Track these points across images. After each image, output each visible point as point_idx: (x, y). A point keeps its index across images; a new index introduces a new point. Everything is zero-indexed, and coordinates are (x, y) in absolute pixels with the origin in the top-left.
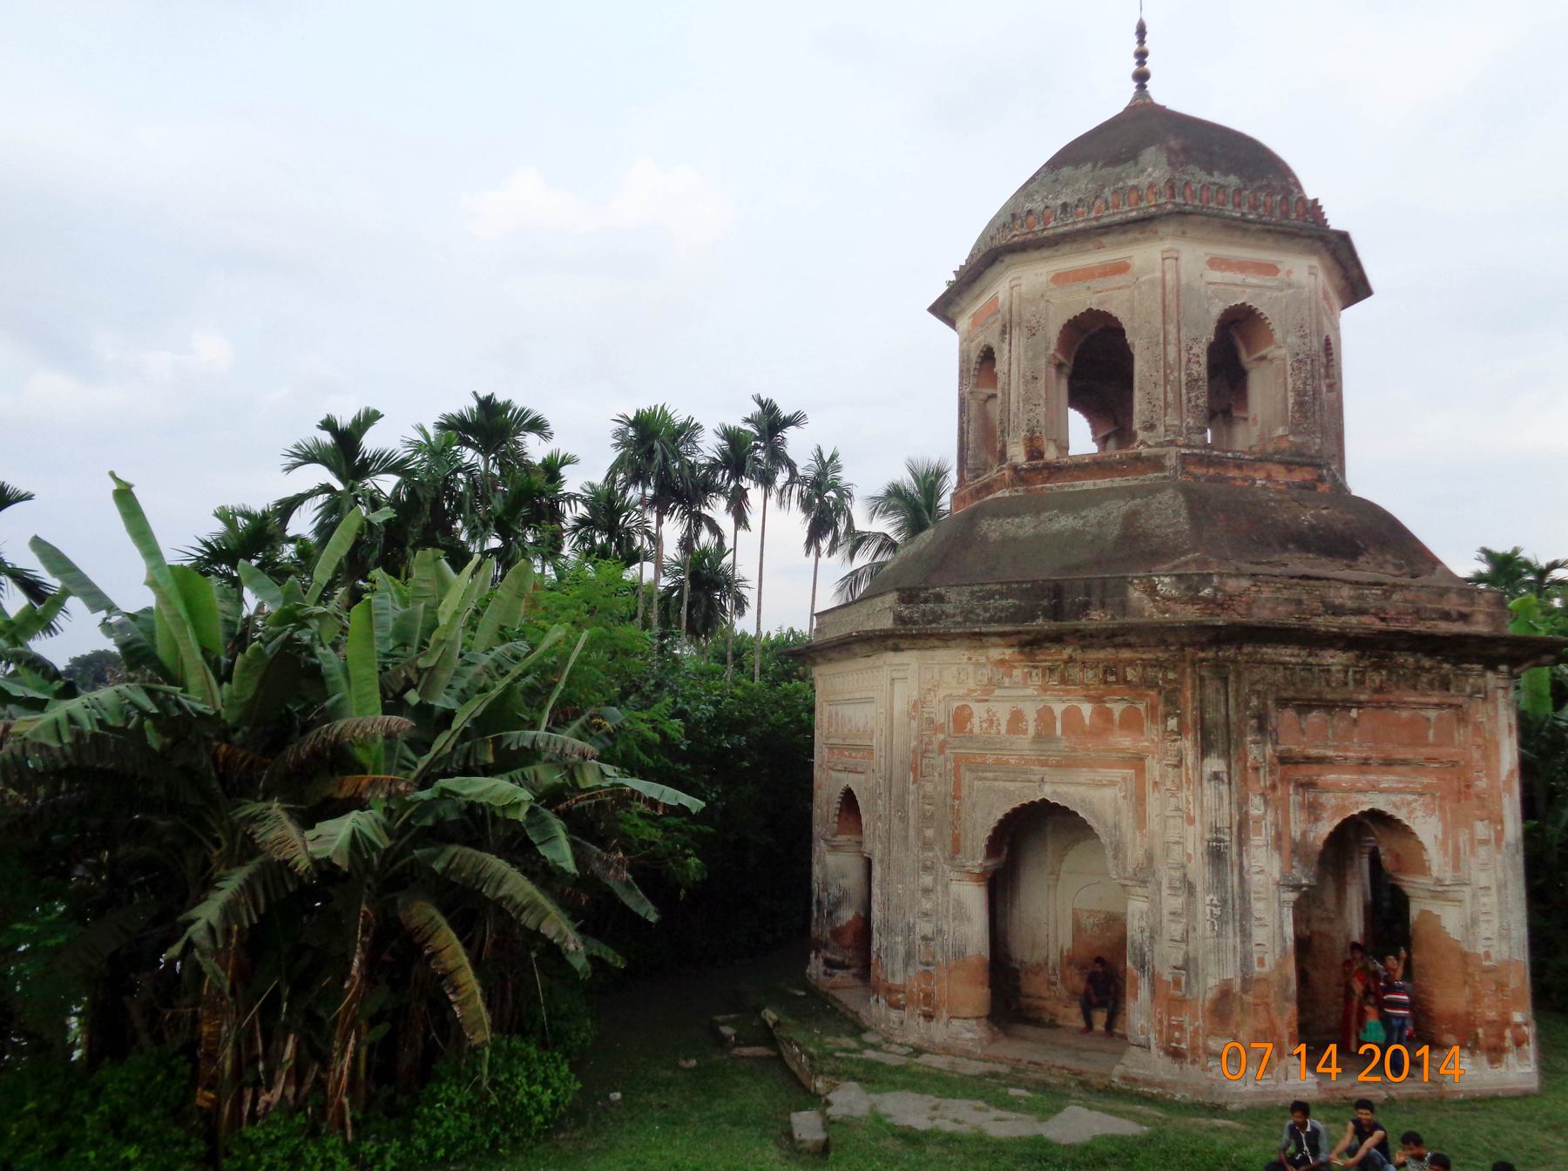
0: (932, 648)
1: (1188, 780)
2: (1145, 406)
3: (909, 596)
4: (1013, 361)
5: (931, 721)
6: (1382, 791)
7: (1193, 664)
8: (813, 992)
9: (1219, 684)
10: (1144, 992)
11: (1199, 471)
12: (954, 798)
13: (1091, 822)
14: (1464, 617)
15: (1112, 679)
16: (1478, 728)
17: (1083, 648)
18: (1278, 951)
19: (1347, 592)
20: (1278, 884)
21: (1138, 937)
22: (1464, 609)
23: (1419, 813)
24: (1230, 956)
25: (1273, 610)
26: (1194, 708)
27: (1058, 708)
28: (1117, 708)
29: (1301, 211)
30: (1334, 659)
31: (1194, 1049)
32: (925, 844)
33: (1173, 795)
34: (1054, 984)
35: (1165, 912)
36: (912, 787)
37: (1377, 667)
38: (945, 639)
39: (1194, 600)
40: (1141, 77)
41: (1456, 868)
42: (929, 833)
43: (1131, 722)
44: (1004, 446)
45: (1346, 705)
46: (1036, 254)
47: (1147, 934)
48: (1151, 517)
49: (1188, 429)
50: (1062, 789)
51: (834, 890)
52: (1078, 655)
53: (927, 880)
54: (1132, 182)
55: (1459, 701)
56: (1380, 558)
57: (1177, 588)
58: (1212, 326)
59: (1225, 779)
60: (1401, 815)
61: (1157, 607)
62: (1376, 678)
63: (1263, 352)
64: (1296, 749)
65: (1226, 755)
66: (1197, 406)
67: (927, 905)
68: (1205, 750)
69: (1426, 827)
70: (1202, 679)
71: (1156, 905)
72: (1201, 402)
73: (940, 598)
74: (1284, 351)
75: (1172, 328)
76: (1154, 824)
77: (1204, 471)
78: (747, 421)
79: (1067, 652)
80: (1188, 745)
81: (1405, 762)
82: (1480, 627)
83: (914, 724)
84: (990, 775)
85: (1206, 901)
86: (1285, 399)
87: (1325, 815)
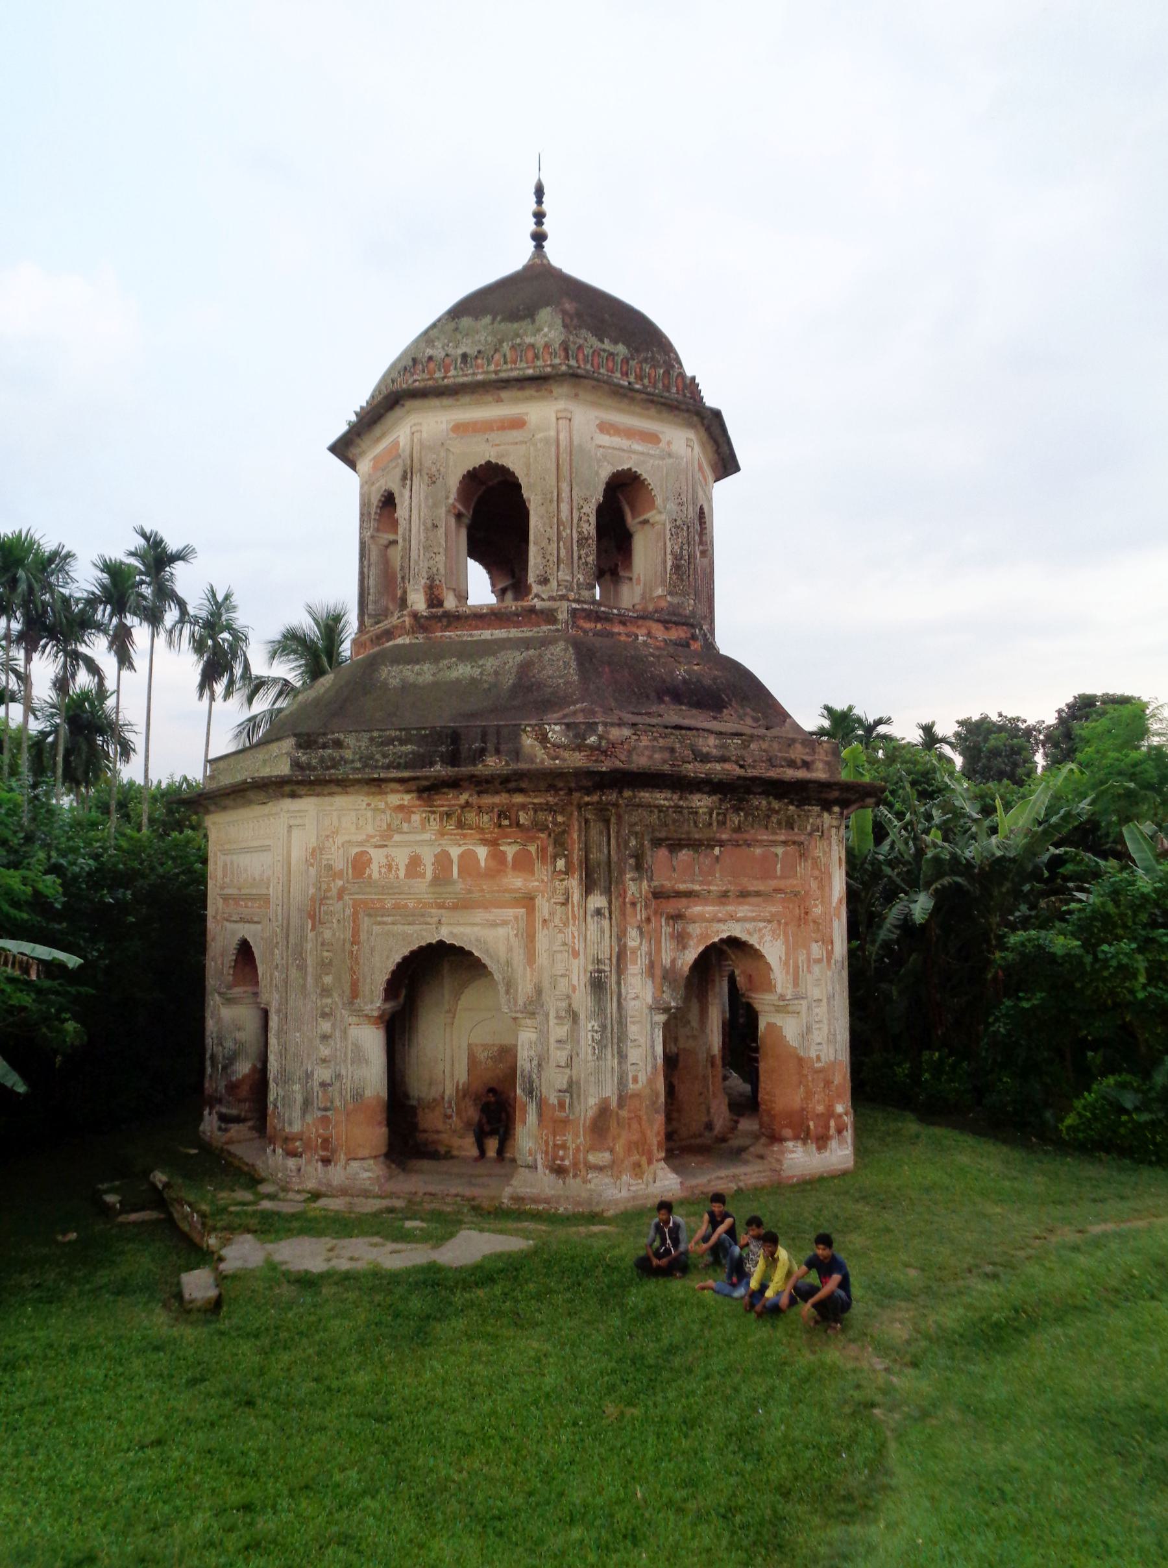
0: (331, 794)
1: (574, 916)
2: (539, 560)
3: (306, 742)
4: (413, 508)
5: (330, 867)
6: (738, 920)
7: (579, 807)
8: (206, 1148)
9: (601, 825)
10: (532, 1117)
11: (588, 625)
12: (353, 943)
13: (486, 960)
14: (806, 765)
15: (506, 822)
16: (815, 861)
17: (479, 793)
18: (649, 1069)
19: (713, 740)
20: (651, 1008)
21: (527, 1066)
22: (808, 758)
23: (768, 938)
24: (609, 1075)
25: (650, 757)
26: (580, 849)
27: (455, 852)
28: (510, 851)
29: (681, 385)
30: (701, 802)
31: (575, 1164)
32: (323, 990)
33: (560, 931)
34: (450, 1117)
35: (552, 1040)
36: (311, 935)
37: (737, 810)
38: (343, 785)
39: (579, 748)
40: (539, 238)
41: (796, 984)
42: (328, 980)
43: (523, 864)
44: (405, 592)
46: (436, 402)
47: (535, 1062)
48: (544, 668)
49: (578, 585)
50: (458, 930)
51: (229, 1044)
52: (474, 800)
53: (326, 1026)
54: (529, 340)
55: (802, 838)
56: (741, 711)
57: (567, 736)
58: (601, 488)
59: (607, 915)
60: (753, 940)
61: (548, 754)
62: (735, 819)
63: (645, 517)
64: (668, 884)
65: (608, 892)
66: (587, 563)
67: (325, 1051)
68: (588, 890)
70: (587, 821)
71: (543, 1034)
72: (590, 559)
73: (338, 744)
74: (663, 517)
75: (565, 487)
76: (542, 959)
77: (593, 625)
78: (132, 554)
79: (464, 797)
80: (574, 884)
81: (758, 894)
82: (820, 774)
83: (312, 871)
84: (389, 919)
85: (587, 1026)
86: (665, 562)
87: (692, 943)
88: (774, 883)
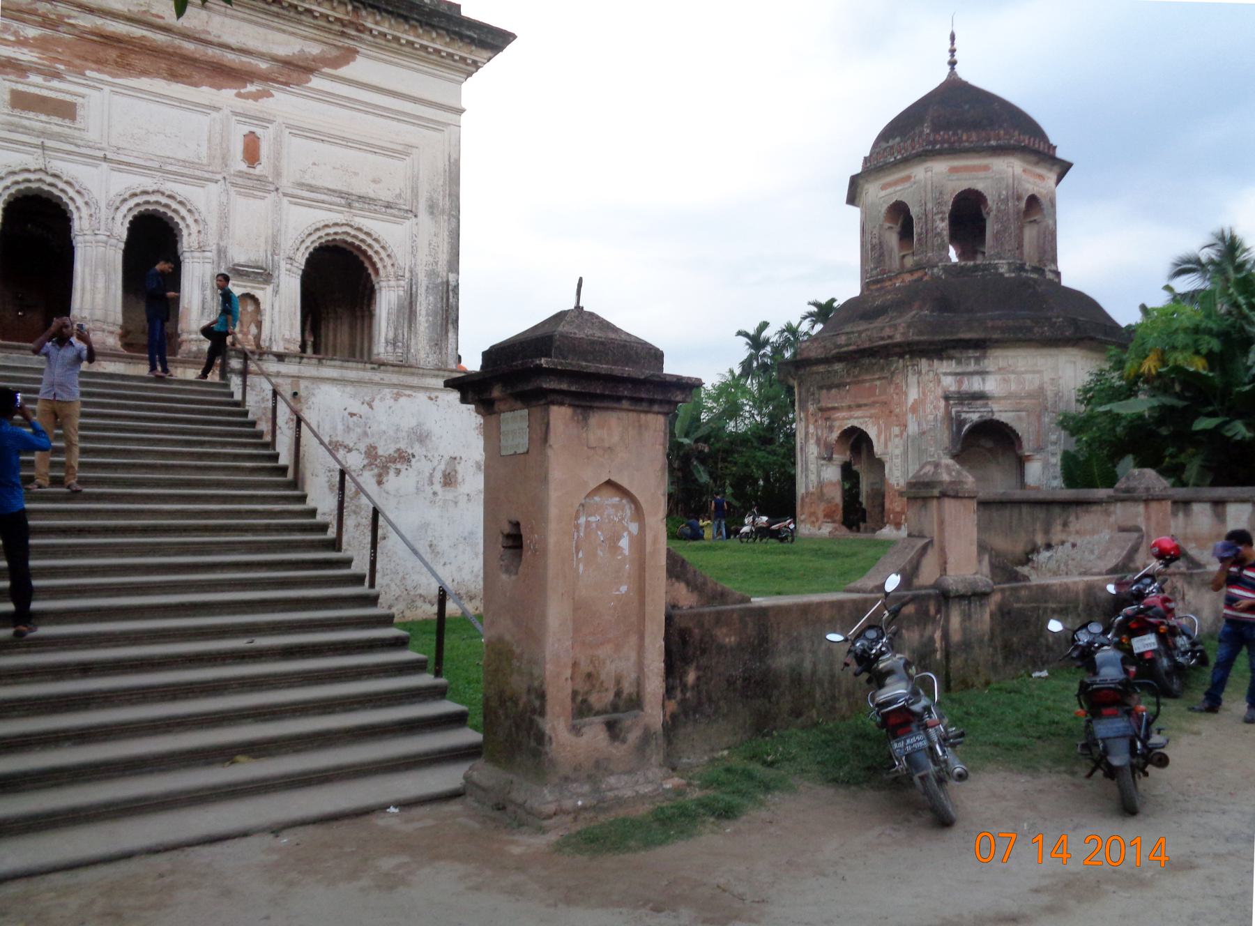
14: (890, 337)
30: (838, 367)
40: (953, 64)
45: (845, 385)
60: (863, 427)
69: (872, 433)
81: (865, 405)
82: (898, 338)
88: (872, 399)
